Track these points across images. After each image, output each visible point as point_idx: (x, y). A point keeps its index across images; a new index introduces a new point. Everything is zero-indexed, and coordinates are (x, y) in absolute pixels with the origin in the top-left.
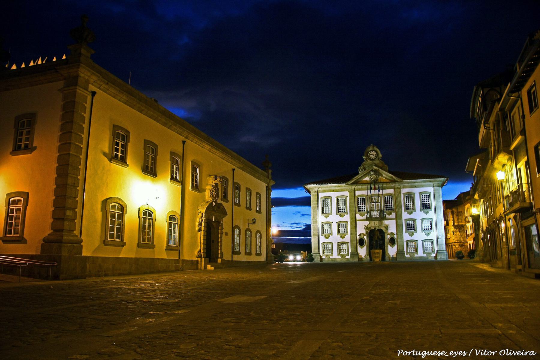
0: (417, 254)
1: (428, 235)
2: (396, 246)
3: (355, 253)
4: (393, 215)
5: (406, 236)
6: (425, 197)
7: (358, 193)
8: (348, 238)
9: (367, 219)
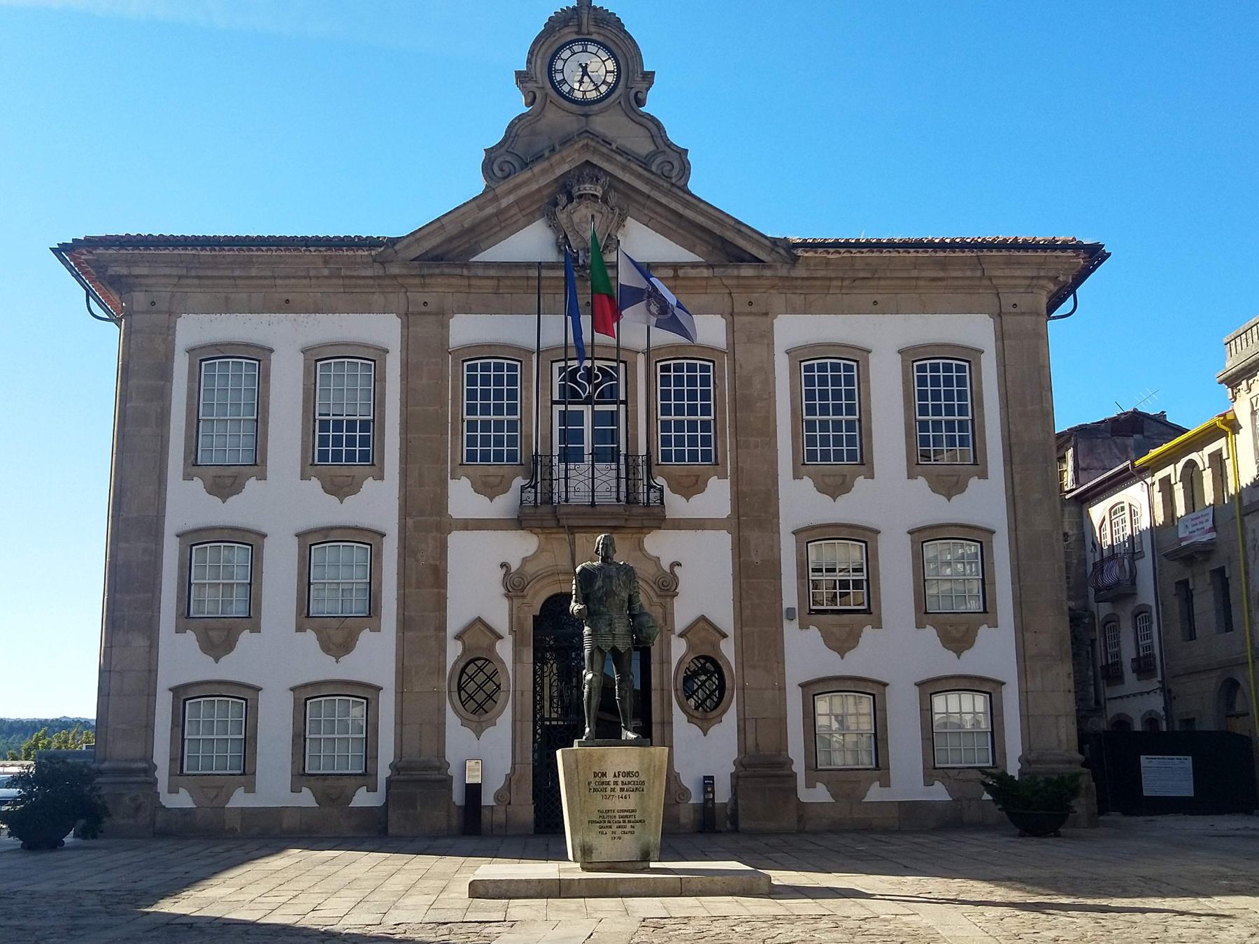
0: (886, 783)
2: (730, 717)
4: (716, 498)
5: (805, 653)
7: (467, 329)
8: (374, 659)
9: (520, 521)
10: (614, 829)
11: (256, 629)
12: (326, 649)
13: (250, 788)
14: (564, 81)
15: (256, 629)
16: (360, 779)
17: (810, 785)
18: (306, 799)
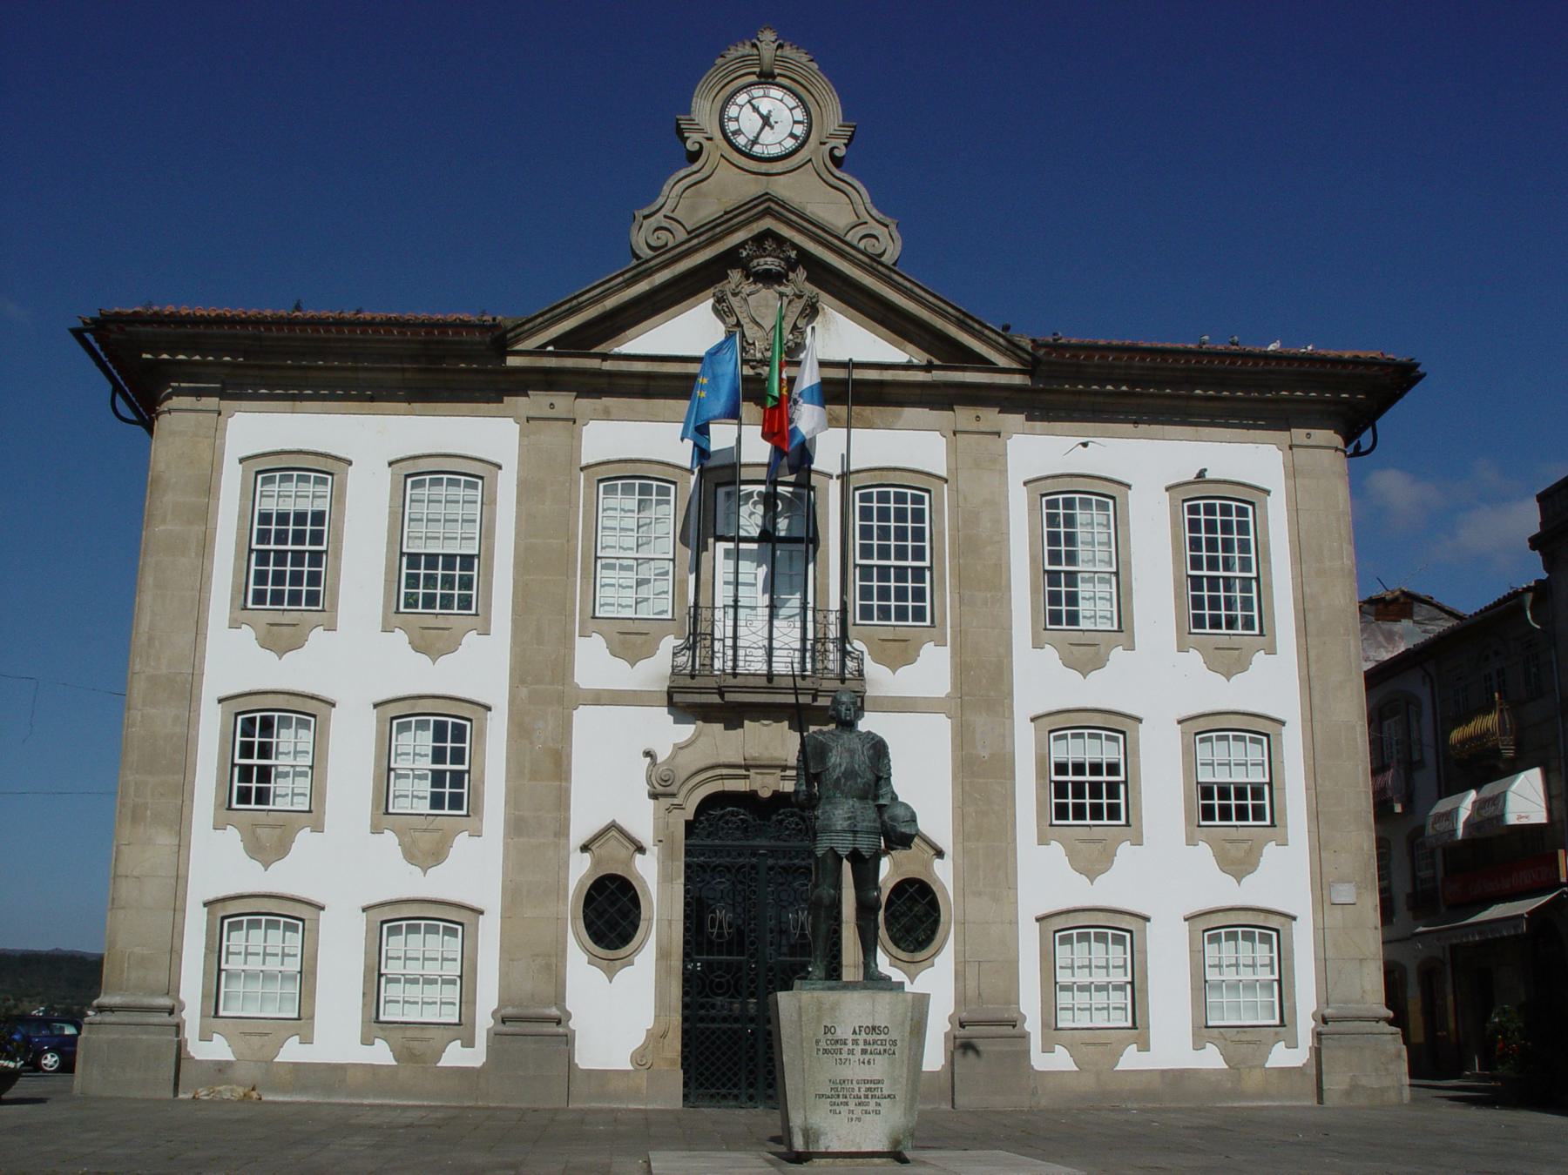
0: (1144, 1046)
1: (1239, 864)
3: (535, 1027)
4: (932, 670)
6: (1215, 528)
8: (475, 868)
10: (852, 1106)
11: (318, 827)
12: (410, 856)
13: (307, 1040)
14: (738, 132)
15: (318, 827)
16: (452, 1032)
17: (1047, 1048)
18: (381, 1054)
